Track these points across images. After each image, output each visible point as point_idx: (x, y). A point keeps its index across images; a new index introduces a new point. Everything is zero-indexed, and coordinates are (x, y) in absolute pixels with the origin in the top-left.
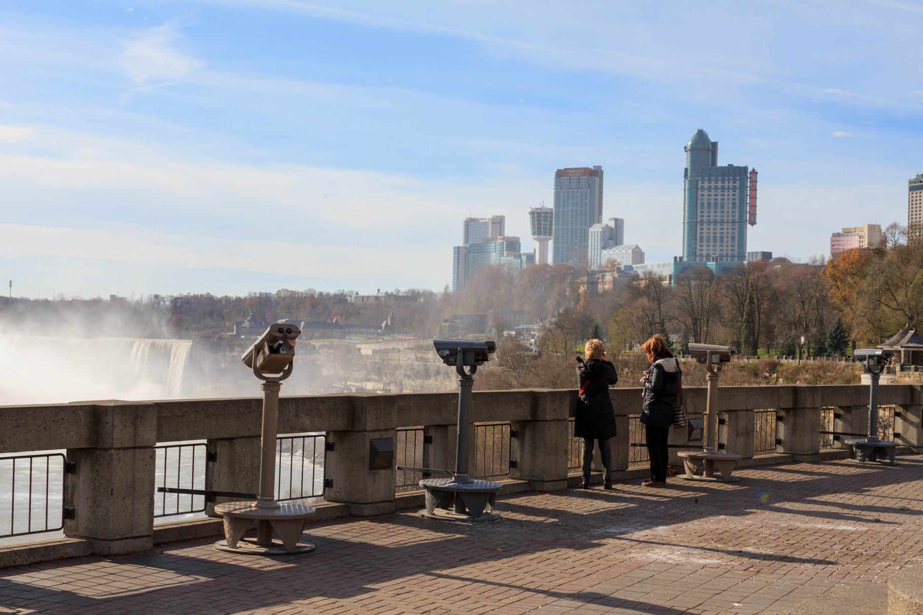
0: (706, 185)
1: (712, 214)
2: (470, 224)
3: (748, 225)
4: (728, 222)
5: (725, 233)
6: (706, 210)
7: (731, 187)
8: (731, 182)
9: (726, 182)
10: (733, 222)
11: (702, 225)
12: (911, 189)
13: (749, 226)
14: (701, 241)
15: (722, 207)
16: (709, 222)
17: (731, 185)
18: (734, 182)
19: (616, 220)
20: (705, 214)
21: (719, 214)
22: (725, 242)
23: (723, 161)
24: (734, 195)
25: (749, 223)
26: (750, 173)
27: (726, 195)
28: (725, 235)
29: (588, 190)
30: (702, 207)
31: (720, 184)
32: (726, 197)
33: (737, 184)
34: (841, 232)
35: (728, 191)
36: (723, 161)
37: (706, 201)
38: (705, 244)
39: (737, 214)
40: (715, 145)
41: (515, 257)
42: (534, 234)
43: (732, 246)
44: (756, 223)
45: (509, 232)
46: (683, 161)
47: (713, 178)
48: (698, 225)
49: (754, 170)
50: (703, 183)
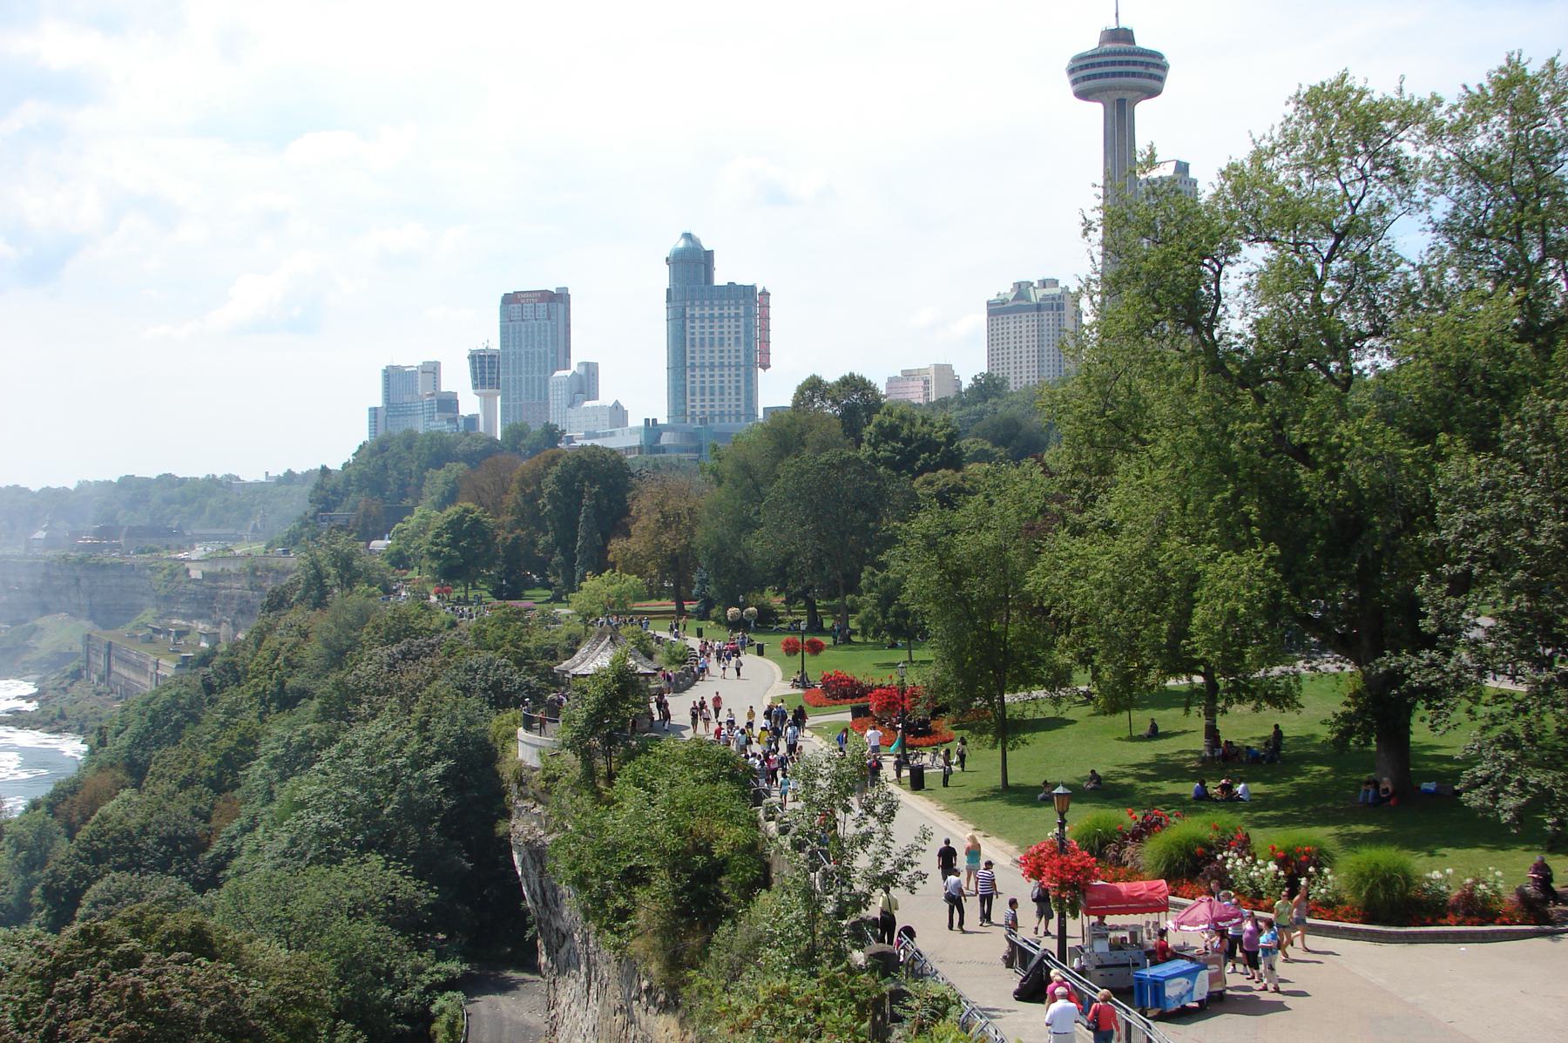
0: (697, 312)
1: (707, 354)
2: (394, 378)
4: (730, 365)
6: (697, 348)
10: (738, 367)
13: (760, 370)
14: (693, 394)
16: (702, 366)
17: (733, 312)
18: (737, 308)
19: (587, 365)
23: (720, 279)
29: (548, 322)
31: (716, 312)
32: (726, 330)
33: (742, 311)
34: (900, 375)
36: (720, 279)
37: (697, 337)
38: (698, 398)
39: (742, 354)
41: (449, 421)
42: (475, 386)
45: (445, 387)
46: (662, 279)
47: (707, 302)
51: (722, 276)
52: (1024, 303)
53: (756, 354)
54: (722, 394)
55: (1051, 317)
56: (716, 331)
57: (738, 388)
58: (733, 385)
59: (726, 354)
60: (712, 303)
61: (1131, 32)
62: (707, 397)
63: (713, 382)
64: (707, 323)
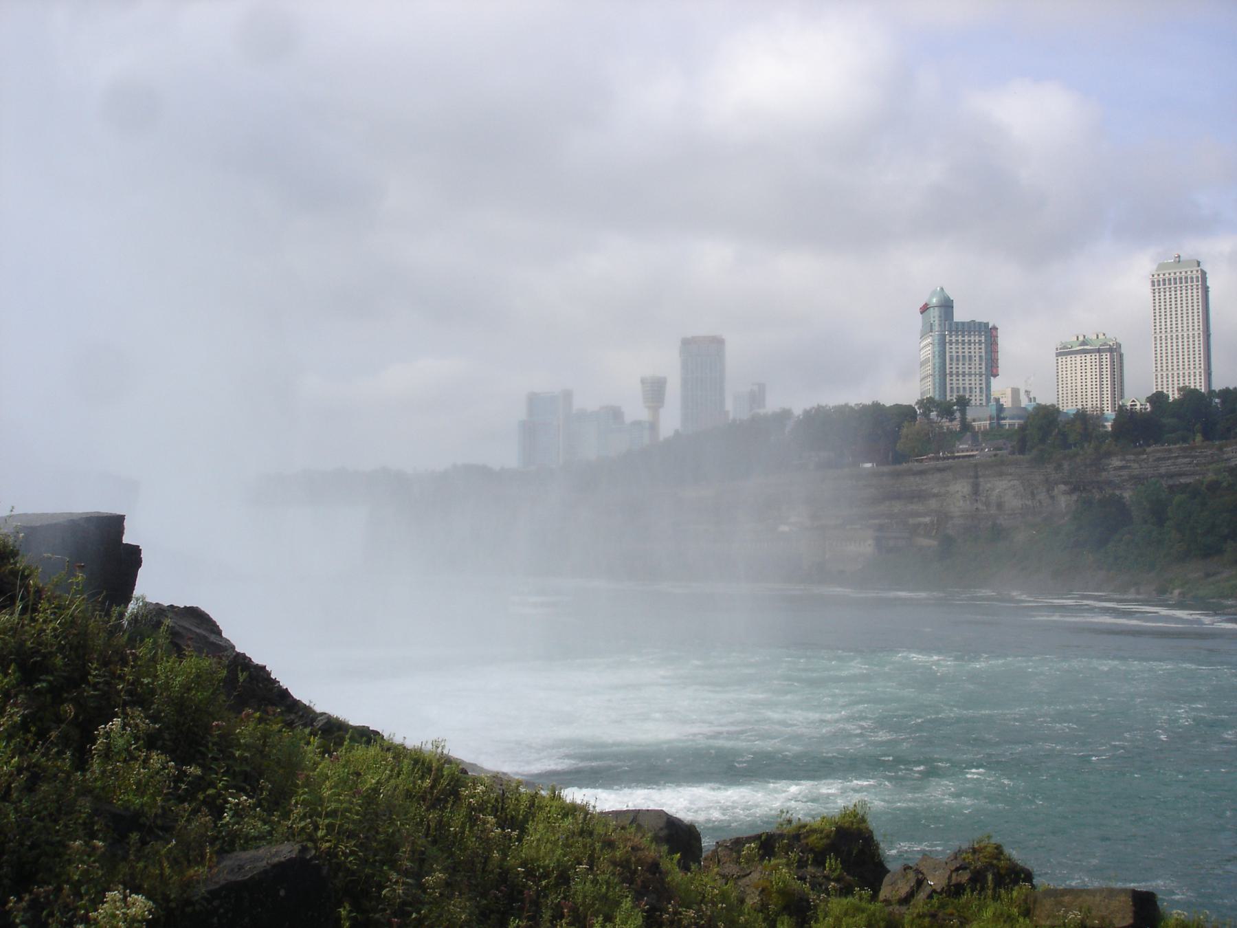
4: (975, 375)
8: (977, 337)
12: (1058, 355)
13: (992, 378)
15: (970, 360)
20: (954, 366)
21: (967, 366)
22: (974, 392)
24: (980, 349)
27: (973, 348)
28: (973, 386)
30: (951, 359)
31: (966, 339)
32: (972, 350)
33: (983, 339)
37: (954, 354)
39: (984, 368)
40: (953, 301)
43: (981, 396)
50: (951, 336)
51: (960, 316)
52: (1086, 347)
53: (992, 369)
55: (1108, 357)
56: (966, 351)
57: (981, 388)
58: (978, 386)
59: (973, 366)
60: (963, 333)
64: (960, 346)
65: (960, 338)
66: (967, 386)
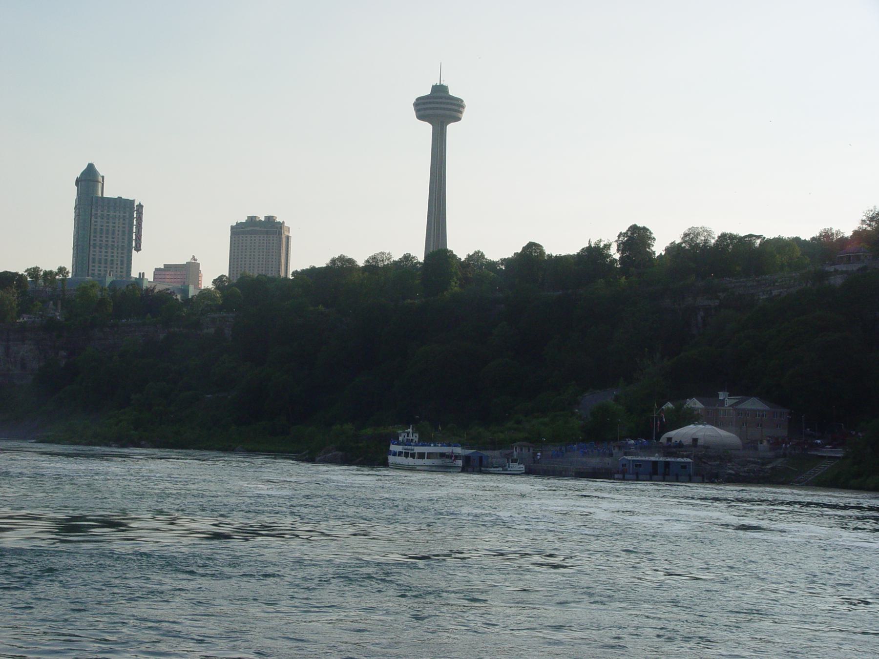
0: (99, 212)
3: (133, 251)
5: (115, 257)
6: (98, 234)
7: (121, 216)
9: (118, 212)
11: (94, 248)
14: (94, 262)
15: (113, 233)
17: (122, 215)
21: (110, 239)
25: (135, 250)
26: (137, 206)
28: (115, 258)
30: (95, 233)
33: (127, 215)
35: (119, 220)
37: (99, 227)
38: (97, 265)
44: (140, 250)
48: (91, 247)
49: (140, 203)
54: (112, 264)
61: (447, 87)
62: (103, 265)
63: (106, 256)
65: (105, 212)
66: (109, 258)
